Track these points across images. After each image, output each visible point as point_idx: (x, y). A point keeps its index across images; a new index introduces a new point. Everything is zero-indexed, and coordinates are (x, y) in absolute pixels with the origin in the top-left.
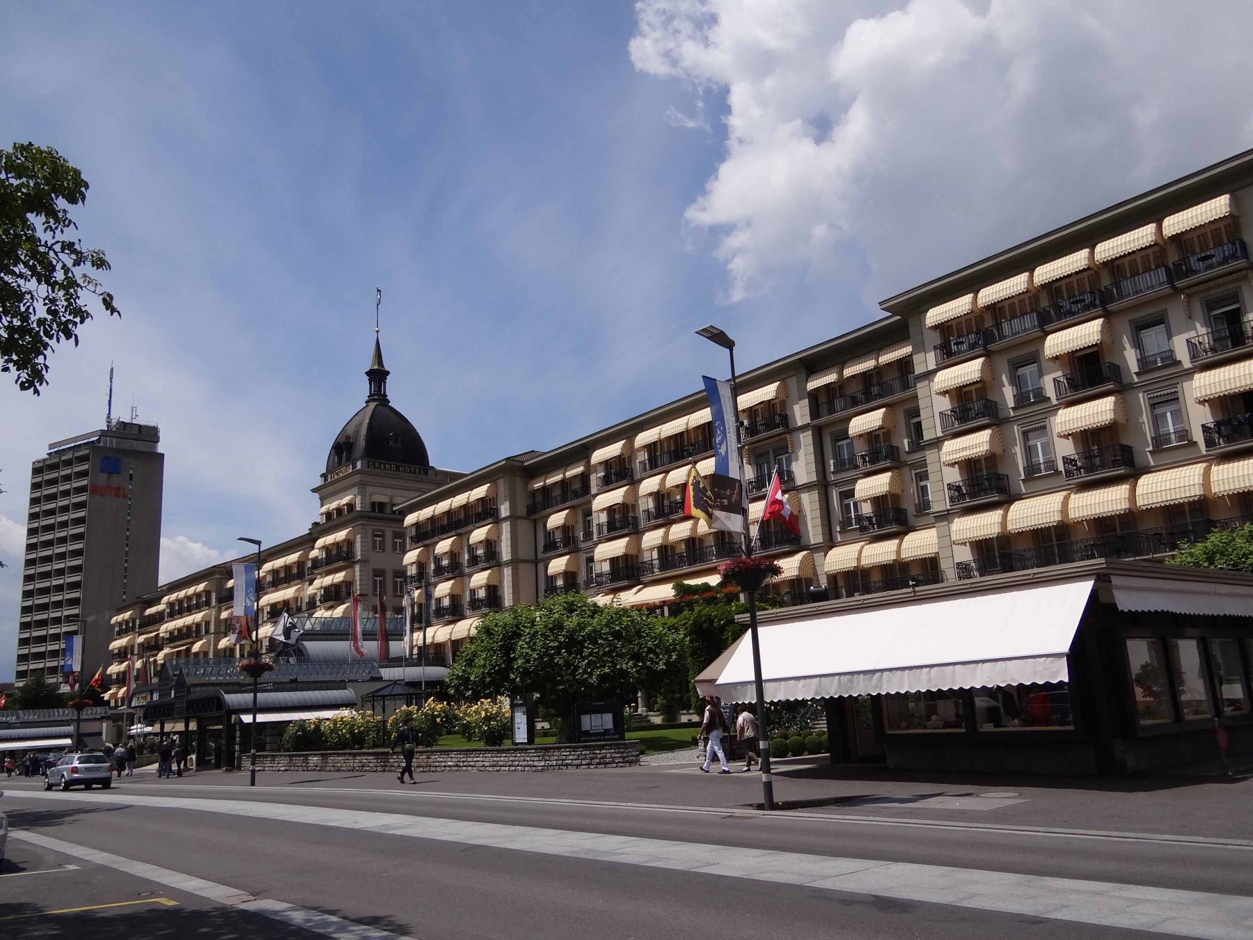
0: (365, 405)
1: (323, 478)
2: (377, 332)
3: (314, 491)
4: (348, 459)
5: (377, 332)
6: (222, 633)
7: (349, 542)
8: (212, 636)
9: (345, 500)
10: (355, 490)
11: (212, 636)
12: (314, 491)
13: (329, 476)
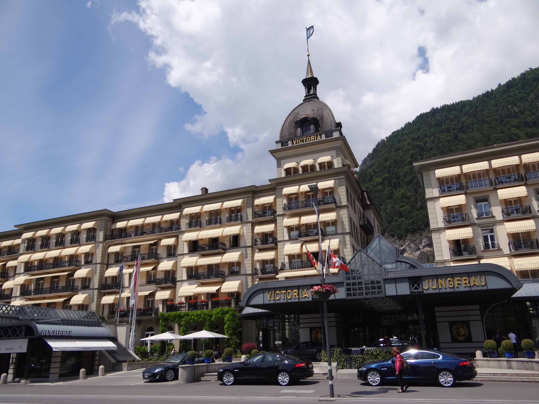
0: (303, 102)
1: (280, 144)
2: (308, 55)
3: (272, 152)
4: (317, 130)
5: (308, 55)
6: (105, 264)
7: (331, 191)
8: (99, 266)
9: (325, 159)
10: (334, 152)
11: (99, 266)
12: (272, 152)
13: (290, 142)
